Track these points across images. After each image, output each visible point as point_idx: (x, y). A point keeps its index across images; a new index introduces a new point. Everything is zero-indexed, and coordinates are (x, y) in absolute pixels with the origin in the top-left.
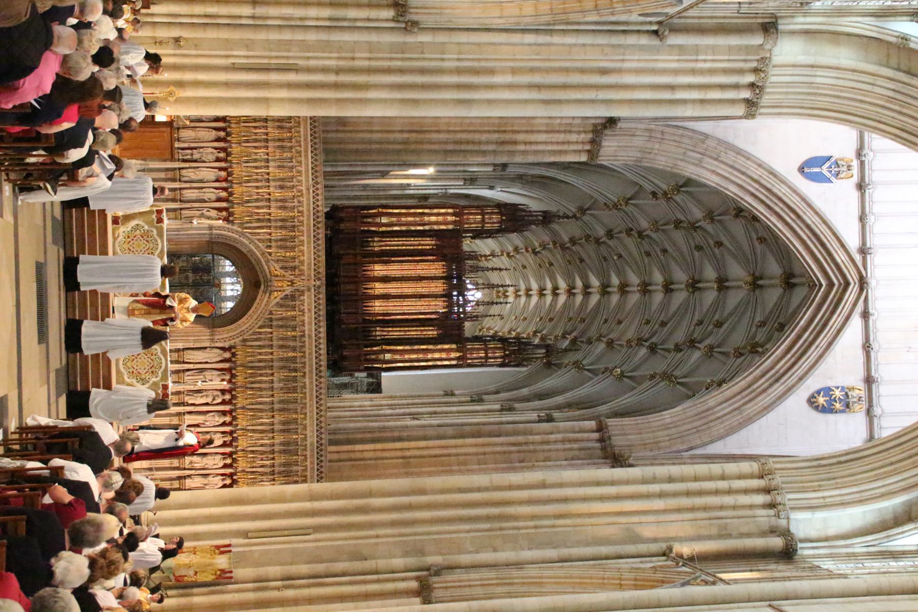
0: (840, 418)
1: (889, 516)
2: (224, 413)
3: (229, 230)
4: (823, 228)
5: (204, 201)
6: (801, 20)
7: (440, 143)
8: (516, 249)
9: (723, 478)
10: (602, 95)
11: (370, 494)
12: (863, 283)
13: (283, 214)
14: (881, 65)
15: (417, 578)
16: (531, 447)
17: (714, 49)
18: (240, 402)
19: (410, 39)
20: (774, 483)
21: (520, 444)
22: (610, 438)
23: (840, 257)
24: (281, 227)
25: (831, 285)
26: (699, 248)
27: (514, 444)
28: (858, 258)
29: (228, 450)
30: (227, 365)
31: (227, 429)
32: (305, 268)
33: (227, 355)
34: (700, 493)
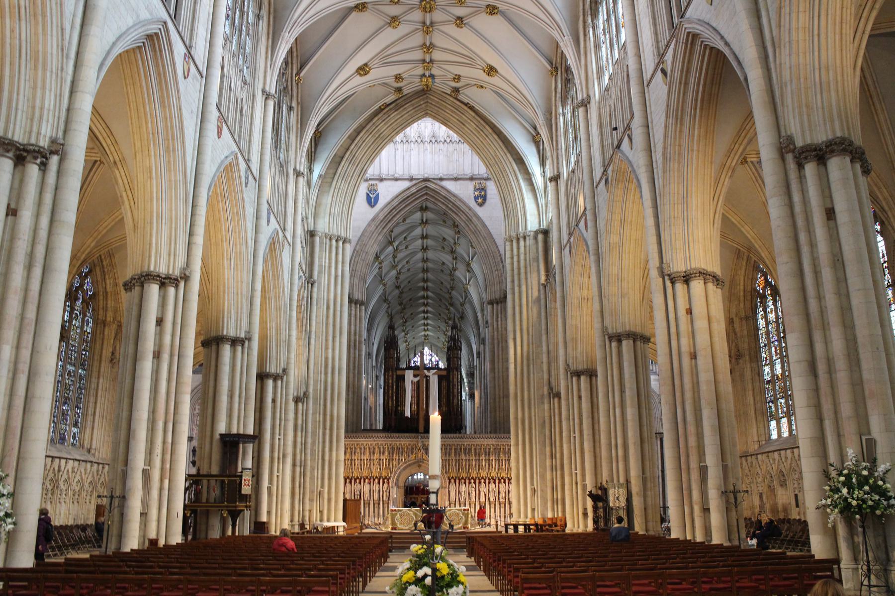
0: (489, 192)
1: (529, 188)
2: (480, 483)
3: (393, 479)
4: (400, 197)
5: (379, 491)
6: (309, 220)
7: (354, 377)
8: (404, 331)
9: (512, 258)
10: (338, 308)
11: (516, 418)
12: (426, 180)
13: (386, 453)
14: (330, 186)
15: (553, 398)
16: (500, 337)
17: (320, 258)
18: (474, 475)
19: (311, 396)
20: (515, 236)
21: (498, 342)
22: (496, 299)
23: (414, 190)
24: (393, 454)
25: (426, 194)
26: (407, 247)
27: (498, 345)
28: (414, 182)
29: (497, 481)
30: (457, 481)
31: (487, 481)
32: (412, 443)
33: (453, 481)
34: (519, 269)
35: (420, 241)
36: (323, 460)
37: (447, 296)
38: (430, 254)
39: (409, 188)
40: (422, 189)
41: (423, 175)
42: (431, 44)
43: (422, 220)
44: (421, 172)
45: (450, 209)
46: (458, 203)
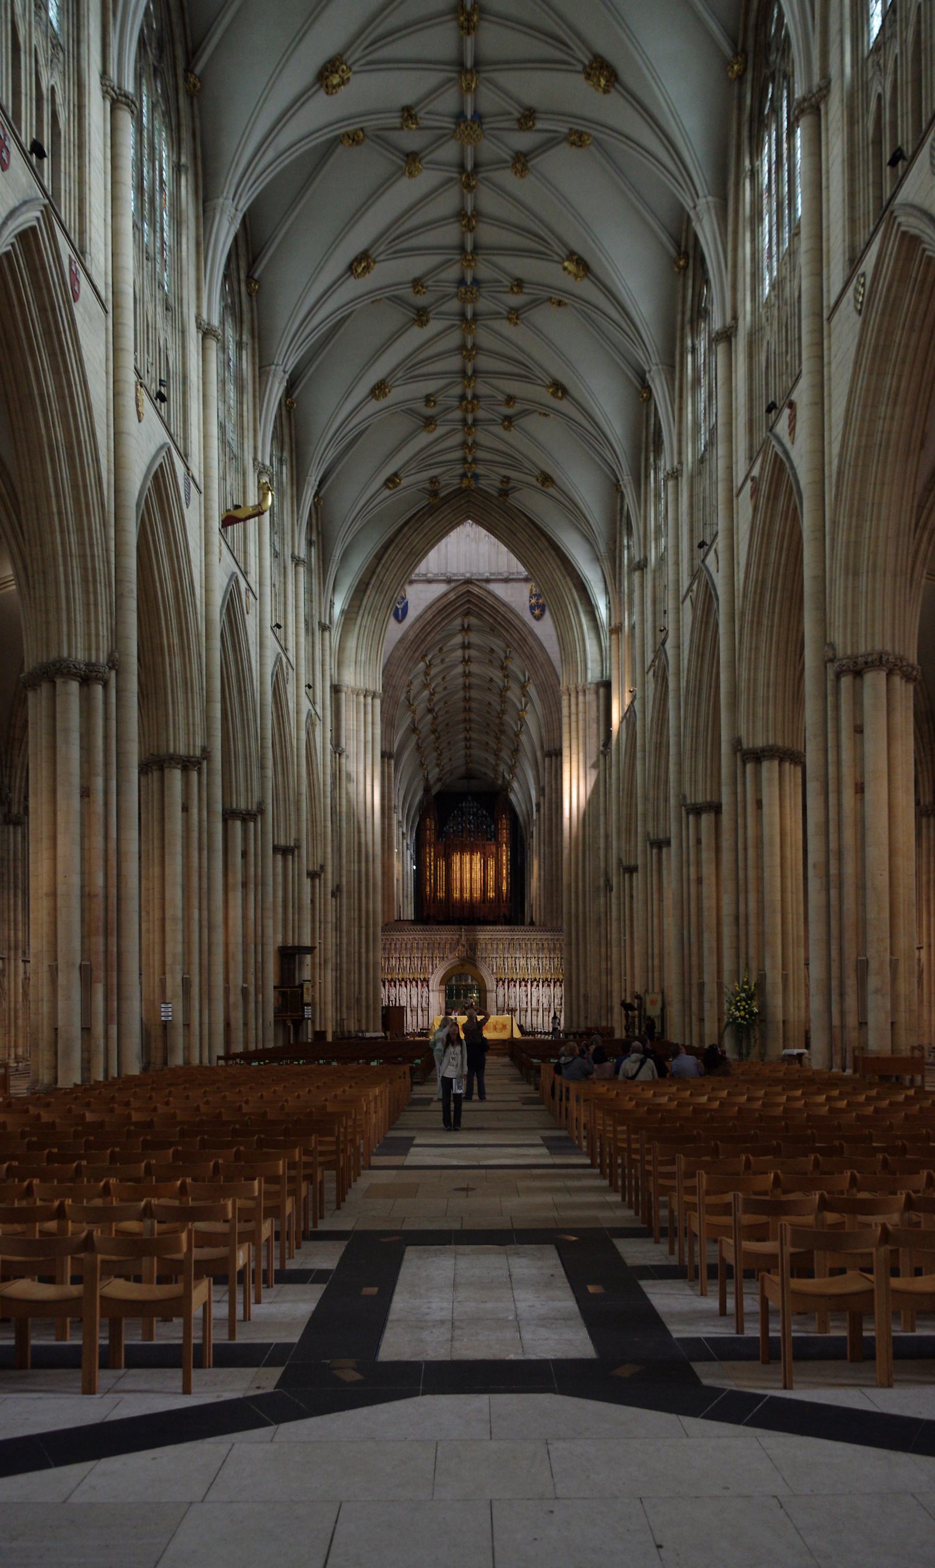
12: (468, 582)
23: (452, 596)
25: (469, 601)
28: (453, 585)
33: (501, 983)
35: (459, 653)
36: (360, 962)
37: (497, 721)
38: (474, 668)
39: (445, 595)
40: (463, 594)
41: (463, 575)
42: (474, 442)
43: (463, 626)
44: (462, 571)
45: (500, 624)
46: (510, 616)
